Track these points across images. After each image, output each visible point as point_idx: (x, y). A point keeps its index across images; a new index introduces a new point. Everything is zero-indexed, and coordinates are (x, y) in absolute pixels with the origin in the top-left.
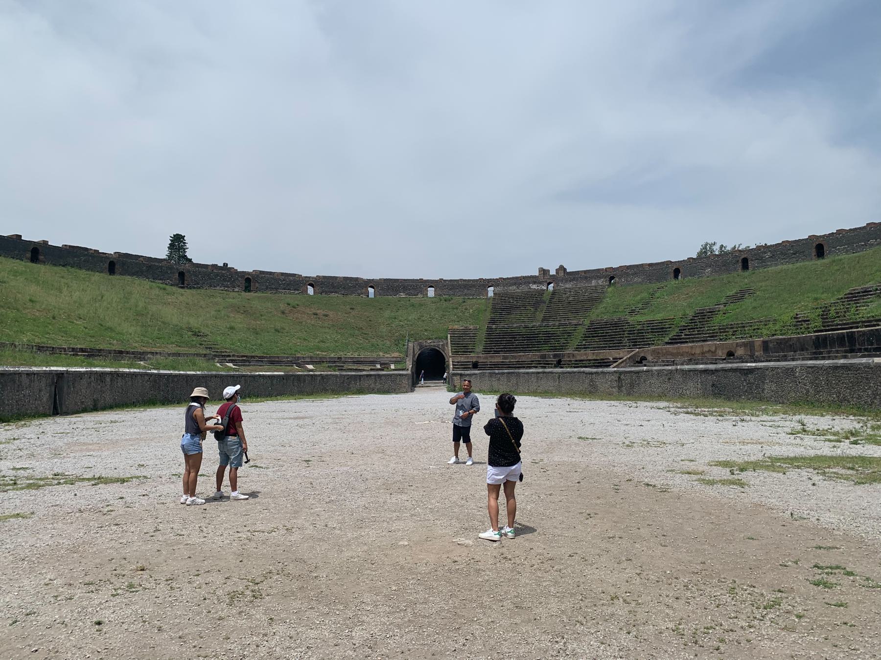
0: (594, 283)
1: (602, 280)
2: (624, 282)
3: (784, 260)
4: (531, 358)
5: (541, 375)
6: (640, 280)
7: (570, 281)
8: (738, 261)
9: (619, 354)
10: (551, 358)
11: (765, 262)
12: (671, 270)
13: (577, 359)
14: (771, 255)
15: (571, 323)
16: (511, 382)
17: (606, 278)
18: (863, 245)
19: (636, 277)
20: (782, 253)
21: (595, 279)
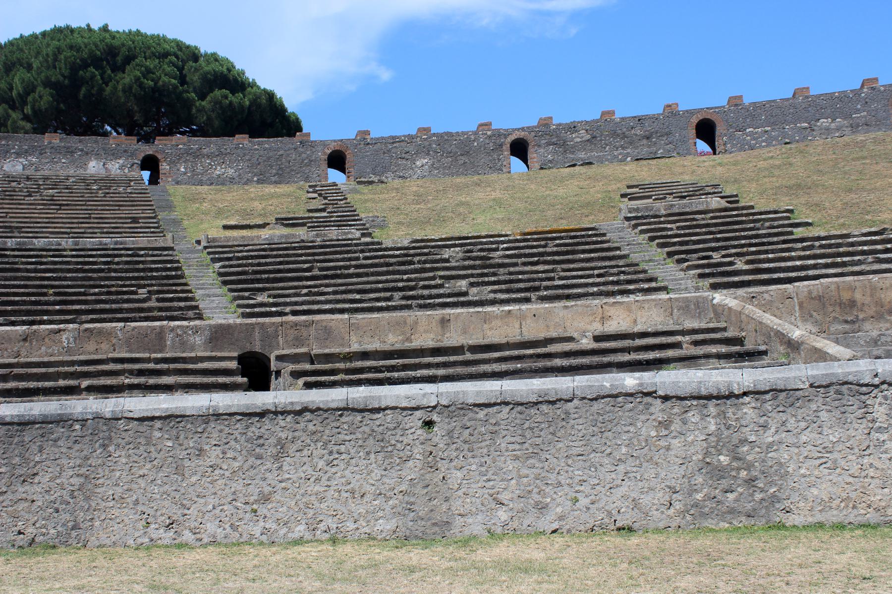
0: (94, 167)
1: (121, 161)
2: (185, 173)
3: (620, 151)
4: (69, 351)
5: (281, 428)
6: (231, 172)
7: (18, 155)
8: (501, 145)
9: (603, 320)
10: (192, 349)
11: (573, 153)
12: (322, 155)
13: (355, 347)
14: (588, 137)
15: (121, 243)
16: (44, 479)
17: (132, 155)
18: (805, 128)
19: (219, 164)
20: (614, 134)
21: (98, 156)
